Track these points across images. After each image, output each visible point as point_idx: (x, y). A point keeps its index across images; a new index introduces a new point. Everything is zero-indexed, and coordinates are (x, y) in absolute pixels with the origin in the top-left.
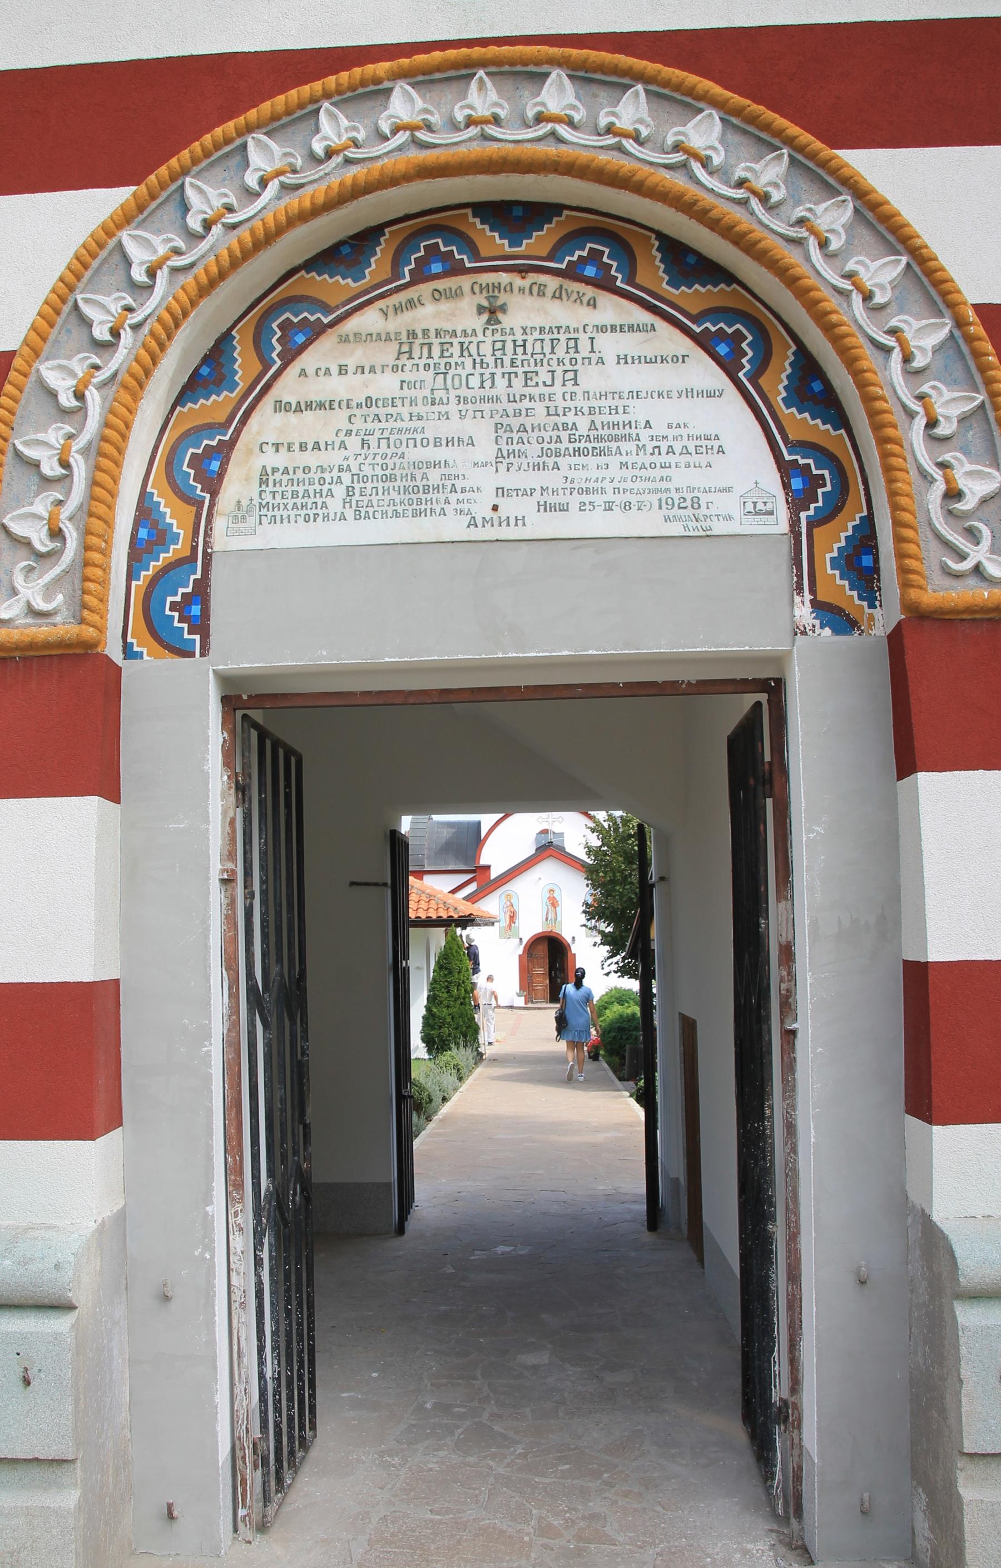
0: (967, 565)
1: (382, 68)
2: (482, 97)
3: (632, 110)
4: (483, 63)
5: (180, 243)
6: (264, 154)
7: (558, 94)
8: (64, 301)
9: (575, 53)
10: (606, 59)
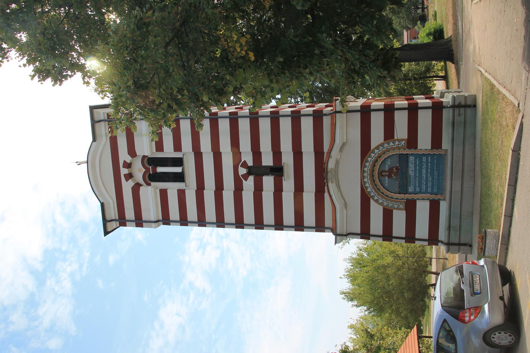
2: (365, 174)
3: (367, 164)
6: (369, 190)
7: (366, 169)
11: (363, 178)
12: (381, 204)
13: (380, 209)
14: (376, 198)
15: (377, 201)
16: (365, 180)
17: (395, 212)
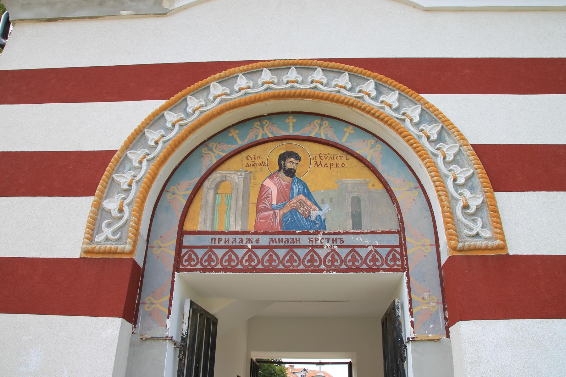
0: (474, 233)
2: (293, 74)
3: (344, 80)
4: (293, 64)
5: (183, 116)
6: (216, 89)
7: (318, 75)
8: (141, 131)
10: (335, 65)
12: (137, 138)
13: (114, 143)
14: (171, 117)
15: (155, 119)
16: (266, 75)
17: (83, 205)
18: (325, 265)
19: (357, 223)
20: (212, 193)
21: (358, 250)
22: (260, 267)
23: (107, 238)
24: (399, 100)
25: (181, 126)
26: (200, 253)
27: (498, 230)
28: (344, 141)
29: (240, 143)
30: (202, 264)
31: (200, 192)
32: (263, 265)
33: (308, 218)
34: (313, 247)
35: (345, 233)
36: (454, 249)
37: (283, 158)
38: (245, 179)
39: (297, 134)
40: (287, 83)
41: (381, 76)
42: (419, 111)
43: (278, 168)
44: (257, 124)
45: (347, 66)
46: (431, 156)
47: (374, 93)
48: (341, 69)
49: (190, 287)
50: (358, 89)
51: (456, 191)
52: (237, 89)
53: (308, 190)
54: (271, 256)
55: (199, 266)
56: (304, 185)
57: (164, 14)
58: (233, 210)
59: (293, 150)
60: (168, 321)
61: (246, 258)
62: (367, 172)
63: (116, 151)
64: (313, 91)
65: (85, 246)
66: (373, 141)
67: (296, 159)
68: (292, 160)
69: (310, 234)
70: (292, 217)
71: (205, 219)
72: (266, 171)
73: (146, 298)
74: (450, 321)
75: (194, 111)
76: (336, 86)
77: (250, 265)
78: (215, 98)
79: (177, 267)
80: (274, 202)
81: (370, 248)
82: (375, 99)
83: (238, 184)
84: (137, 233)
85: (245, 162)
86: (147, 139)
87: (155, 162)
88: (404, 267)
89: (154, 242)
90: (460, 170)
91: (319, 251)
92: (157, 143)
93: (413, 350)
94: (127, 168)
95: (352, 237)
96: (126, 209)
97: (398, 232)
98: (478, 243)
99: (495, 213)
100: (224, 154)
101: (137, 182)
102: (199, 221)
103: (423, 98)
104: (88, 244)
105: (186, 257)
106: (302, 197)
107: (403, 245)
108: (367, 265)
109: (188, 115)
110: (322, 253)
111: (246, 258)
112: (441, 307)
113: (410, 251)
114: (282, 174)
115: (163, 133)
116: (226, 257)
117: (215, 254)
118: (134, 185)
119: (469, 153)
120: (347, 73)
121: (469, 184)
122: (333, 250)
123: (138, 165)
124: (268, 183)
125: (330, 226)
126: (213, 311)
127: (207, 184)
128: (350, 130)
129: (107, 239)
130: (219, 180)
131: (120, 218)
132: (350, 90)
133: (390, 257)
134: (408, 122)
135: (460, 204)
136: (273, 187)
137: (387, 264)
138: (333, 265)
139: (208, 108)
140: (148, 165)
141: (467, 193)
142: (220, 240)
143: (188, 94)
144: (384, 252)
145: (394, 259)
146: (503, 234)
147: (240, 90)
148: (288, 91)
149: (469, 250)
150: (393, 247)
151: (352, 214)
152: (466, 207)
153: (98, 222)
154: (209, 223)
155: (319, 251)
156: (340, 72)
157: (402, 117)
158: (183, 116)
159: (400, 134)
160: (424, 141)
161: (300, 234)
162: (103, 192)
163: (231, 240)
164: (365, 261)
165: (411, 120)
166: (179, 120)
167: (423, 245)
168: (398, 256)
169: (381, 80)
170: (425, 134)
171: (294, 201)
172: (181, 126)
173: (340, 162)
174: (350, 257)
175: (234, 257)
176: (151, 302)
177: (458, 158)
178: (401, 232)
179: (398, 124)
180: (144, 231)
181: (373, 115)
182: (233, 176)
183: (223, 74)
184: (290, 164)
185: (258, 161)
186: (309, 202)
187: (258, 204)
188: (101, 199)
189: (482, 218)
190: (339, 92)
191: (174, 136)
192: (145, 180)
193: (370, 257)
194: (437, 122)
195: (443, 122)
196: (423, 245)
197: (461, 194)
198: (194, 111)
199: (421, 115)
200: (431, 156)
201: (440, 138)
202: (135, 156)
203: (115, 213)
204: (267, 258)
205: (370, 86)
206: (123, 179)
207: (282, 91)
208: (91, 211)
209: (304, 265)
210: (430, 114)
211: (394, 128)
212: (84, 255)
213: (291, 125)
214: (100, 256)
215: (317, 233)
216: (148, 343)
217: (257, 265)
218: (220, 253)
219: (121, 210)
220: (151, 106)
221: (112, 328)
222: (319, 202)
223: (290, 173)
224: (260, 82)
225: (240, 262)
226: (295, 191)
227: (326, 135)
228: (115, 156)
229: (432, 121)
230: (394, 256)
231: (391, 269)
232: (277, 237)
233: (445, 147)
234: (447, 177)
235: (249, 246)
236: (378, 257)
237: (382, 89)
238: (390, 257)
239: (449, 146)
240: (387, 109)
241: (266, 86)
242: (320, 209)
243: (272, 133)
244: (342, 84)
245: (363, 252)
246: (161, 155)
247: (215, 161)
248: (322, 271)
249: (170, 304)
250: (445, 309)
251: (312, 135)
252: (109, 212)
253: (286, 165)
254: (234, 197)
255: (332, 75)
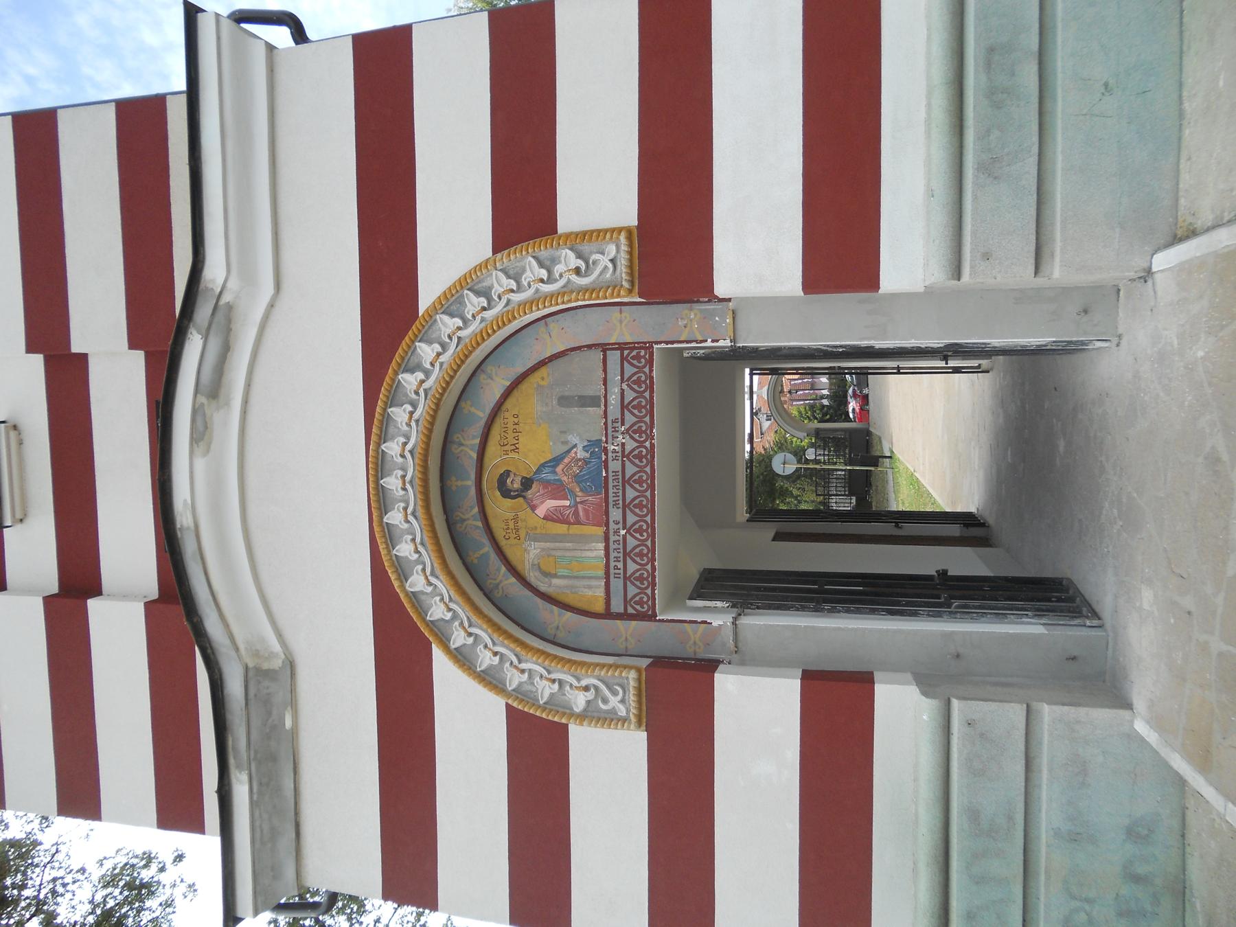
0: (610, 265)
1: (376, 529)
2: (392, 482)
3: (400, 414)
5: (457, 623)
6: (417, 582)
7: (392, 448)
9: (374, 438)
11: (379, 501)
12: (491, 680)
13: (494, 709)
14: (459, 639)
15: (462, 659)
16: (395, 517)
17: (580, 738)
18: (646, 441)
19: (592, 401)
20: (555, 581)
21: (626, 402)
22: (648, 519)
23: (621, 702)
24: (430, 342)
25: (470, 626)
26: (632, 590)
27: (608, 236)
28: (483, 415)
29: (488, 548)
30: (647, 588)
31: (554, 595)
32: (646, 515)
33: (586, 462)
34: (623, 456)
35: (606, 417)
36: (630, 291)
37: (506, 493)
38: (535, 540)
39: (473, 476)
40: (404, 489)
41: (394, 364)
42: (446, 318)
43: (521, 500)
44: (459, 528)
45: (378, 410)
46: (509, 308)
47: (420, 376)
48: (383, 416)
49: (675, 600)
50: (414, 396)
51: (556, 281)
52: (416, 556)
53: (550, 461)
54: (635, 506)
55: (649, 591)
56: (543, 465)
57: (291, 665)
58: (578, 554)
59: (496, 480)
60: (715, 624)
61: (637, 535)
62: (524, 386)
63: (507, 704)
64: (417, 455)
65: (632, 727)
66: (482, 377)
67: (508, 476)
68: (509, 481)
69: (606, 459)
70: (586, 481)
71: (590, 587)
72: (526, 514)
73: (689, 651)
74: (713, 298)
75: (450, 610)
76: (409, 425)
77: (646, 531)
78: (430, 584)
79: (651, 617)
80: (567, 503)
81: (625, 386)
82: (427, 374)
83: (543, 549)
84: (616, 666)
85: (512, 541)
86: (491, 667)
87: (523, 653)
88: (648, 347)
89: (620, 646)
90: (528, 273)
91: (628, 448)
92: (495, 654)
93: (745, 341)
94: (529, 687)
95: (610, 408)
96: (584, 683)
97: (604, 351)
98: (623, 261)
99: (586, 236)
100: (503, 569)
101: (549, 672)
102: (593, 594)
103: (427, 310)
104: (630, 723)
105: (638, 607)
106: (559, 469)
107: (621, 347)
108: (645, 391)
109: (455, 616)
110: (630, 445)
111: (637, 535)
112: (697, 306)
113: (628, 338)
114: (529, 494)
115: (481, 646)
116: (638, 559)
117: (634, 573)
118: (553, 676)
119: (504, 259)
120: (389, 410)
121: (548, 263)
122: (628, 430)
123: (526, 675)
124: (541, 511)
125: (597, 433)
126: (694, 574)
127: (543, 588)
128: (466, 406)
129: (623, 701)
130: (537, 574)
131: (596, 688)
132: (414, 405)
133: (635, 362)
134: (460, 333)
135: (574, 278)
136: (548, 505)
137: (644, 367)
138: (645, 432)
139: (444, 591)
140: (526, 661)
141: (559, 268)
142: (616, 568)
143: (424, 620)
144: (629, 370)
145: (638, 357)
146: (613, 230)
147: (417, 551)
148: (419, 489)
149: (631, 274)
150: (623, 359)
151: (582, 406)
152: (577, 271)
153: (603, 715)
154: (594, 583)
155: (628, 448)
156: (387, 419)
157: (455, 340)
158: (457, 623)
159: (478, 344)
160: (488, 314)
161: (607, 472)
162: (564, 714)
163: (616, 554)
164: (640, 394)
165: (459, 328)
166: (464, 628)
167: (621, 322)
168: (634, 353)
169: (399, 365)
170: (479, 313)
171: (565, 478)
172: (470, 626)
173: (511, 420)
174: (636, 412)
175: (637, 550)
176: (694, 647)
177: (511, 272)
178: (605, 348)
179: (466, 346)
180: (610, 660)
181: (452, 377)
182: (532, 556)
183: (393, 577)
184: (515, 484)
185: (511, 525)
186: (566, 460)
187: (569, 523)
188: (572, 715)
189: (592, 253)
190: (417, 421)
191: (486, 632)
192: (547, 663)
193: (635, 387)
194: (462, 296)
195: (462, 288)
196: (621, 322)
197: (561, 276)
198: (450, 610)
199: (452, 316)
200: (509, 308)
201: (485, 293)
202: (514, 679)
203: (590, 695)
204: (637, 510)
205: (409, 380)
206: (545, 690)
207: (419, 496)
208: (589, 725)
209: (646, 466)
210: (450, 303)
211: (471, 352)
212: (644, 728)
213: (459, 483)
214: (644, 708)
215: (606, 450)
216: (740, 645)
217: (646, 522)
218: (632, 567)
219: (586, 689)
220: (442, 666)
221: (726, 685)
222: (566, 448)
223: (527, 483)
224: (406, 526)
225: (643, 543)
226: (551, 477)
227: (474, 437)
228: (515, 704)
229: (460, 301)
230: (633, 358)
231: (650, 362)
232: (611, 499)
233: (497, 289)
234: (537, 290)
235: (623, 532)
236: (635, 378)
237: (411, 364)
238: (635, 362)
239: (496, 285)
240: (442, 359)
241: (411, 518)
242: (575, 446)
243: (472, 508)
244: (407, 416)
245: (630, 395)
246: (512, 646)
247: (513, 580)
248: (652, 445)
249: (695, 622)
250: (698, 301)
251: (475, 456)
252: (588, 702)
253: (518, 489)
254: (559, 553)
255: (391, 430)
